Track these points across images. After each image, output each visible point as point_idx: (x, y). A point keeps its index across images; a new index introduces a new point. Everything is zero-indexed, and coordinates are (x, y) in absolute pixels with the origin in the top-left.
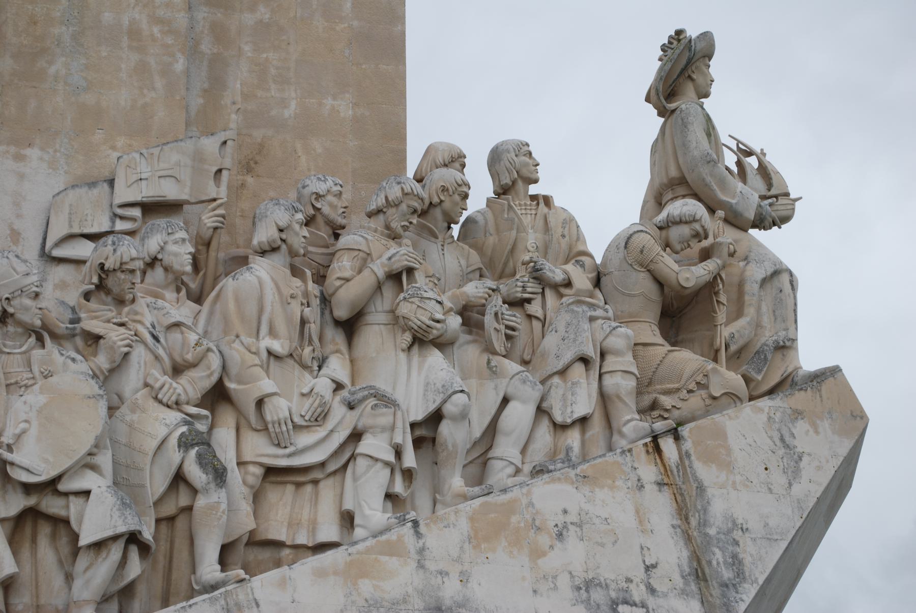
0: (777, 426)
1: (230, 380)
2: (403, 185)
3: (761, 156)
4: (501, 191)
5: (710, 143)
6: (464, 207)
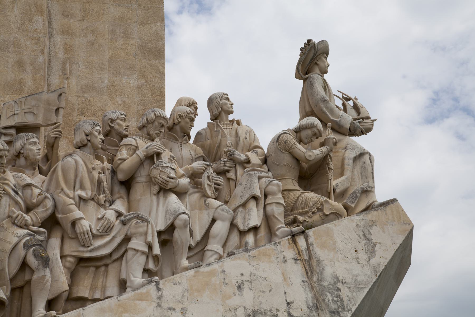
0: (362, 229)
1: (59, 214)
2: (155, 112)
3: (355, 100)
4: (214, 118)
5: (326, 93)
6: (192, 125)
